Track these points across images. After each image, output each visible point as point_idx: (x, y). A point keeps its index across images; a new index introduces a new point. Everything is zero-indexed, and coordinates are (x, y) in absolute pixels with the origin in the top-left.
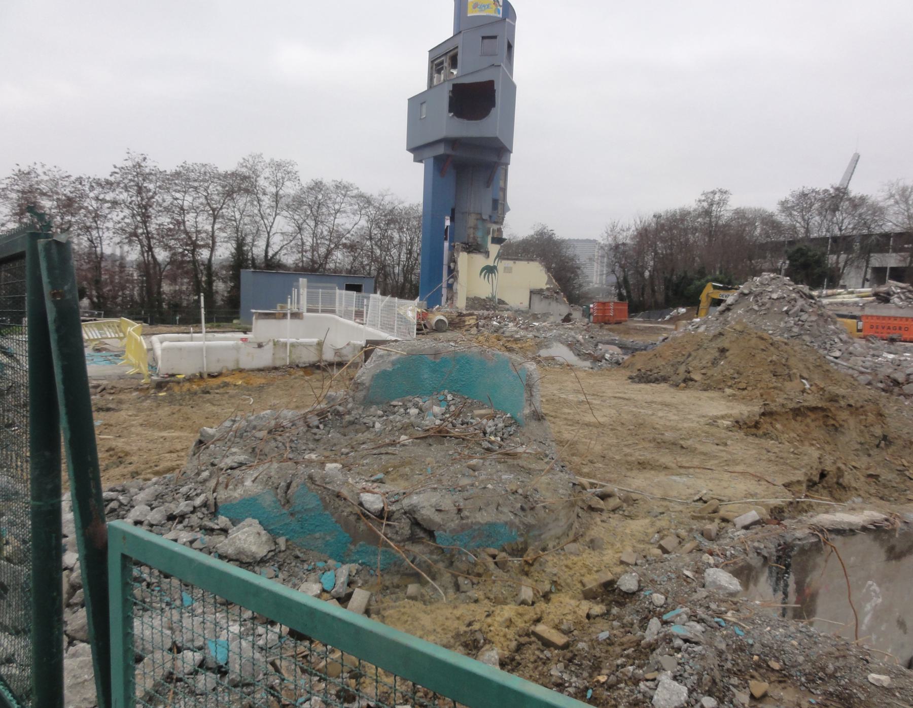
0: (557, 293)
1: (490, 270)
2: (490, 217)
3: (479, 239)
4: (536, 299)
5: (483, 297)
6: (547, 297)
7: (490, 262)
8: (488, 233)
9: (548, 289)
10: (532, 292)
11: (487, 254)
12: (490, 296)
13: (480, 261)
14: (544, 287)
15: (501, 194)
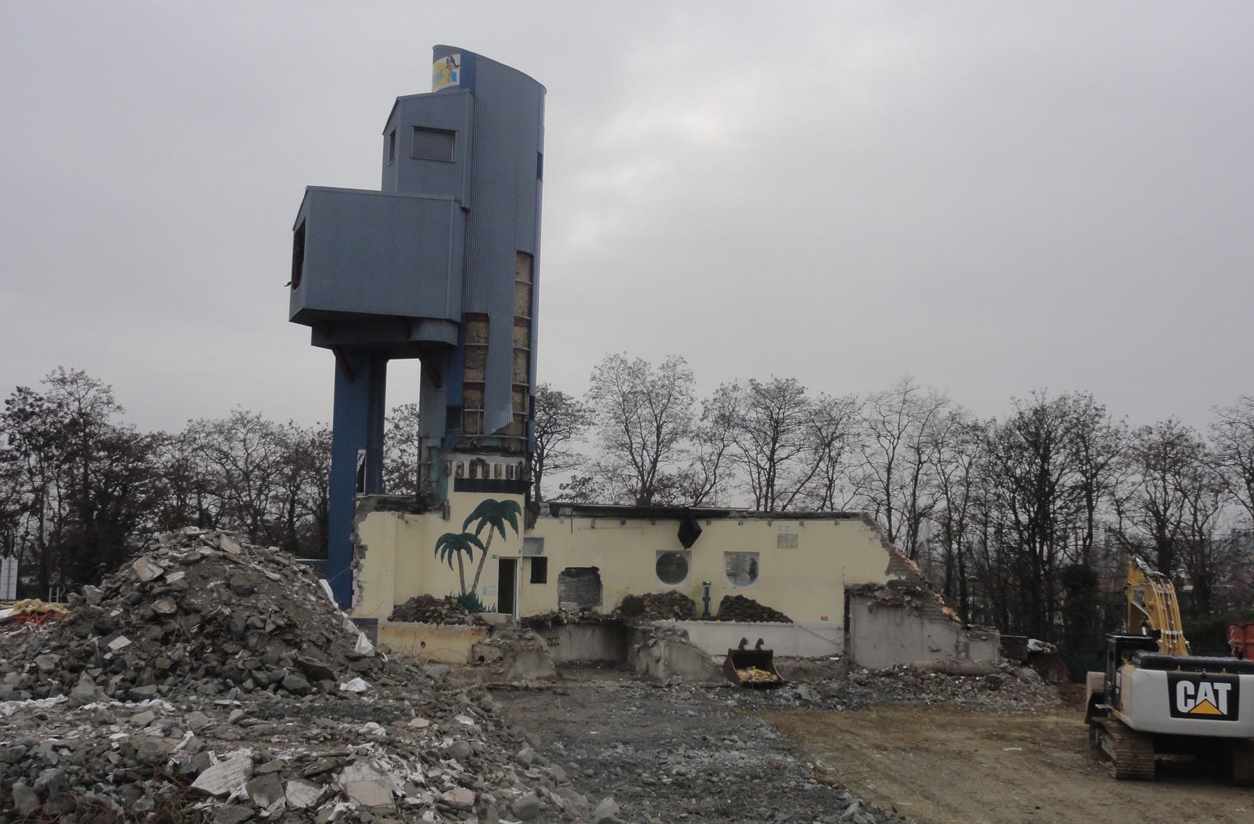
0: (912, 593)
1: (454, 544)
2: (443, 440)
3: (434, 485)
4: (861, 608)
5: (440, 595)
6: (881, 605)
7: (455, 527)
8: (446, 472)
9: (892, 584)
10: (854, 594)
11: (445, 512)
12: (457, 592)
13: (434, 526)
14: (883, 580)
15: (474, 395)
